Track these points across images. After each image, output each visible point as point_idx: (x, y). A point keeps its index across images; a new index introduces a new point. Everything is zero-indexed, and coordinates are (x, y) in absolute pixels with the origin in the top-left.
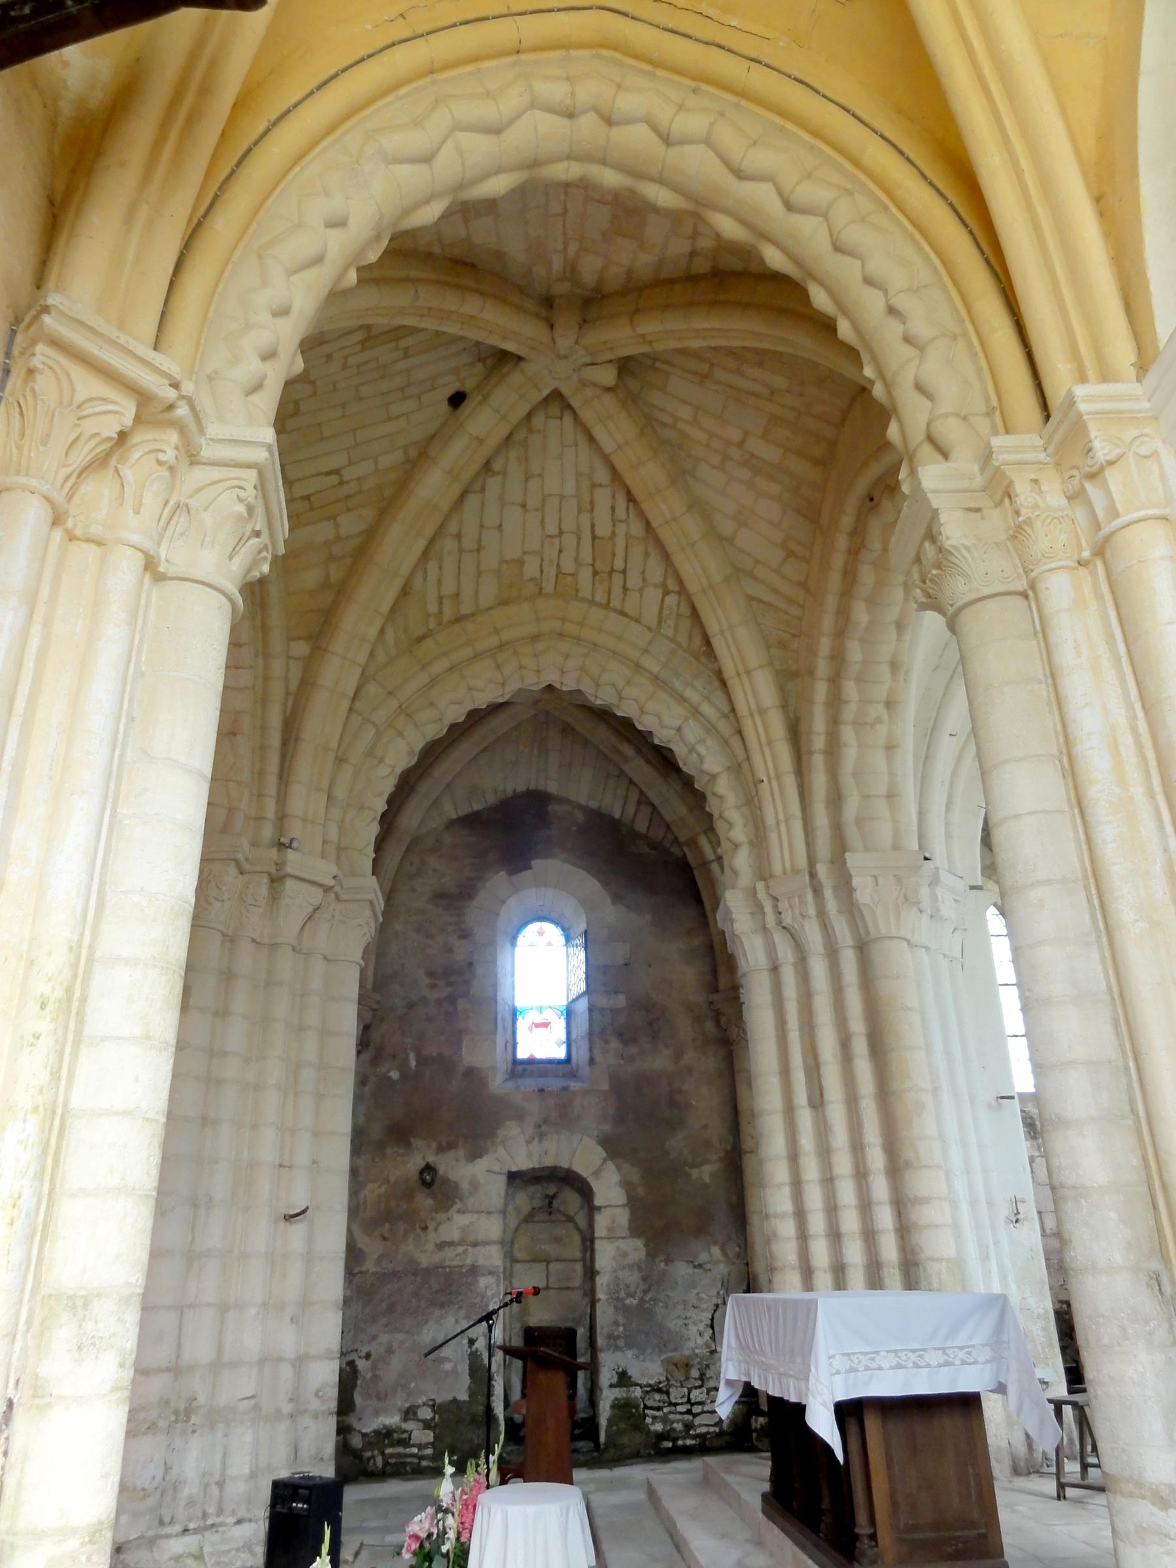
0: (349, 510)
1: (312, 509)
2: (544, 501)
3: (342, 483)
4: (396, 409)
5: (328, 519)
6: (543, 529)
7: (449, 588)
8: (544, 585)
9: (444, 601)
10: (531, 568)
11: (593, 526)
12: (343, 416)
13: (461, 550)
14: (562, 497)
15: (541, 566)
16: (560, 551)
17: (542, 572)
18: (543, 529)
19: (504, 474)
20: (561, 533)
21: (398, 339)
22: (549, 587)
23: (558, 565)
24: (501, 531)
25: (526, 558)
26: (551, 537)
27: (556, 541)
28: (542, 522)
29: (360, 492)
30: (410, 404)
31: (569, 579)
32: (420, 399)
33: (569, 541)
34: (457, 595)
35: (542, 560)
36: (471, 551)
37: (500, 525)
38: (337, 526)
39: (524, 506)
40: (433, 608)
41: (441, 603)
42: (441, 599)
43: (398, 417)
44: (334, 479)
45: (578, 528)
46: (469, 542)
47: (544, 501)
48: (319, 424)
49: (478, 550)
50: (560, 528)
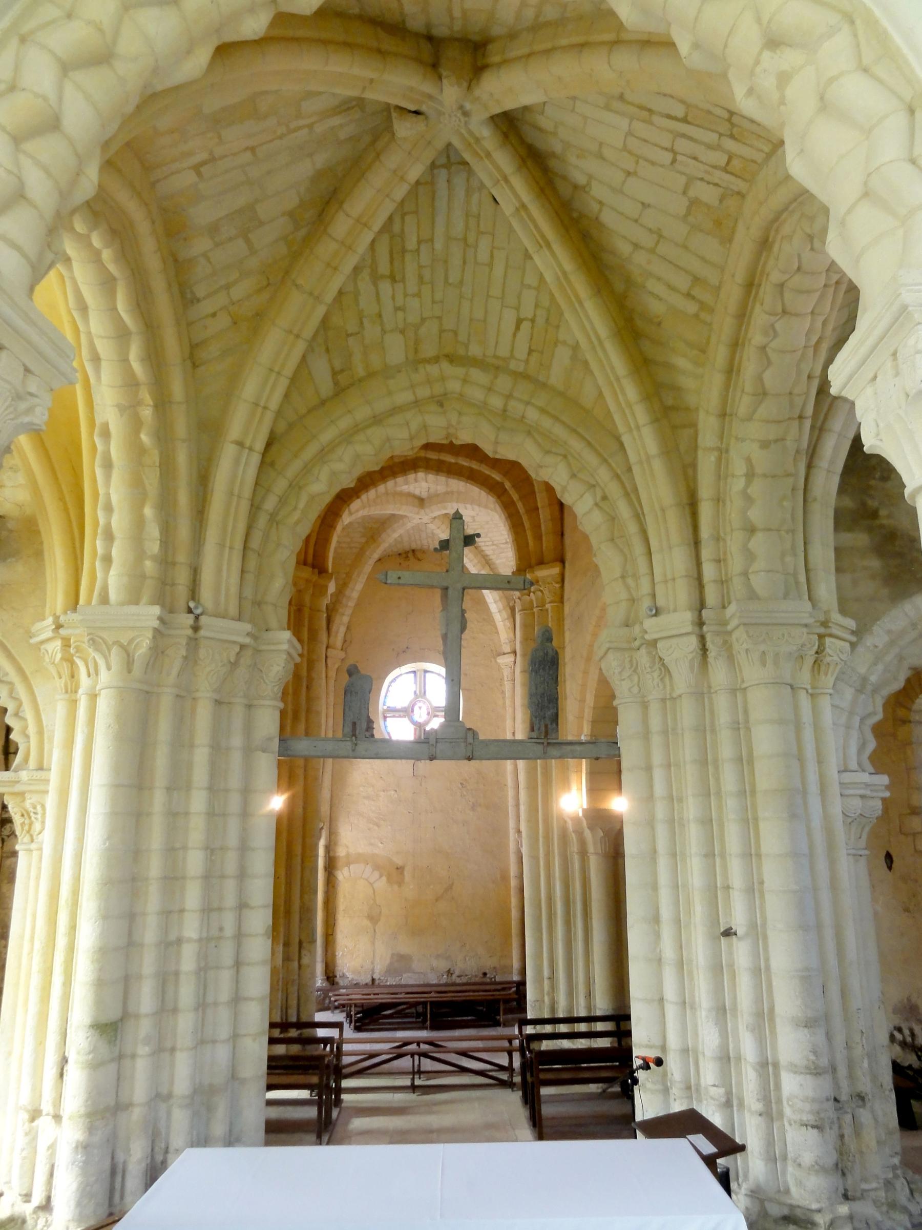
0: (558, 327)
1: (542, 353)
2: (630, 152)
3: (533, 321)
4: (483, 255)
5: (556, 344)
6: (662, 166)
7: (683, 282)
8: (735, 188)
9: (693, 293)
10: (708, 194)
11: (669, 117)
12: (472, 301)
13: (652, 251)
14: (630, 133)
15: (709, 183)
16: (695, 159)
17: (716, 185)
18: (662, 166)
19: (590, 177)
20: (672, 150)
21: (404, 251)
22: (741, 185)
23: (715, 167)
24: (649, 206)
25: (691, 193)
26: (674, 161)
27: (679, 158)
28: (653, 163)
29: (548, 310)
30: (484, 244)
31: (735, 162)
32: (483, 233)
33: (682, 145)
34: (696, 280)
35: (702, 179)
36: (657, 243)
37: (643, 204)
38: (564, 343)
39: (629, 174)
40: (691, 308)
41: (693, 298)
42: (689, 296)
43: (492, 257)
44: (526, 326)
45: (671, 131)
46: (647, 240)
47: (630, 152)
48: (471, 320)
49: (661, 236)
50: (666, 149)
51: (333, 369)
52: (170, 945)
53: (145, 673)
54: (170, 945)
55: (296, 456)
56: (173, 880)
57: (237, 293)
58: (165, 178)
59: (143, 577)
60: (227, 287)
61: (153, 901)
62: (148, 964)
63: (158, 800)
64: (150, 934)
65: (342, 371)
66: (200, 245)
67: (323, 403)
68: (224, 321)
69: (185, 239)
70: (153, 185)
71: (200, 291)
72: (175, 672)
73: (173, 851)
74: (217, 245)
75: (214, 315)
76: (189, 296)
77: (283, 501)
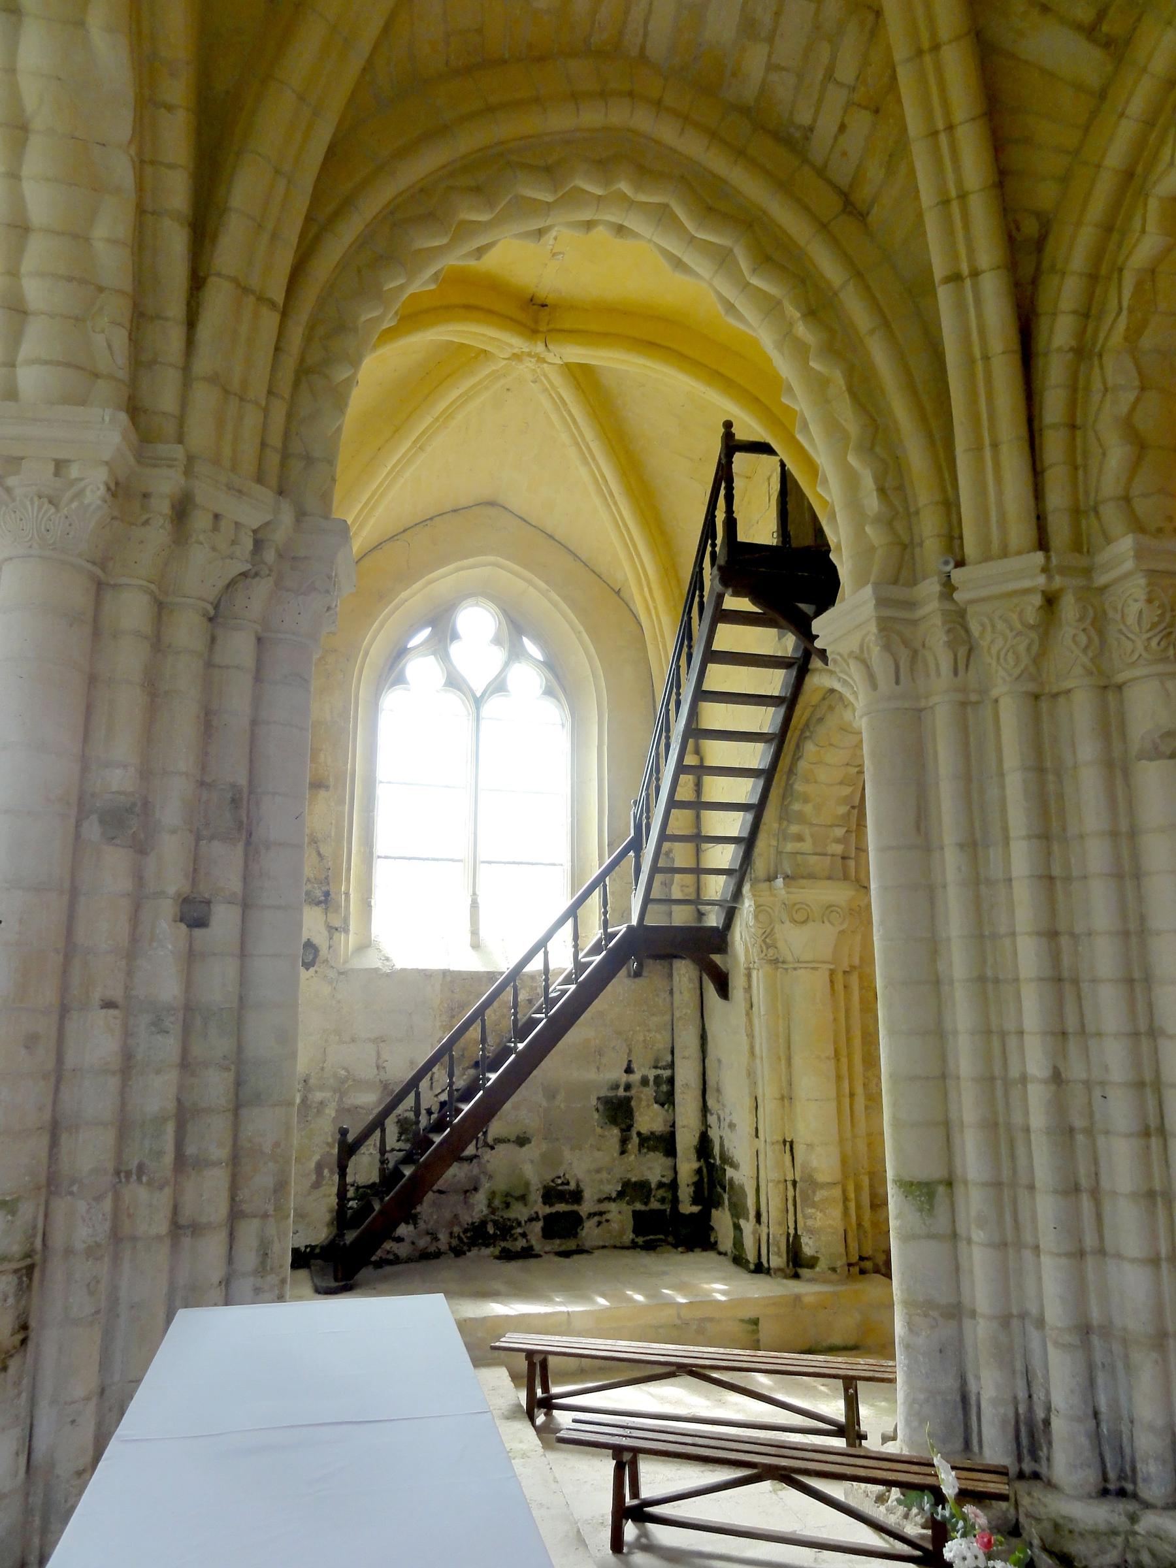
51: (1079, 27)
52: (998, 1083)
53: (897, 682)
54: (998, 1083)
55: (1079, 224)
56: (989, 984)
57: (846, 72)
58: (645, 35)
59: (872, 549)
60: (829, 76)
61: (962, 1015)
62: (968, 1107)
63: (951, 863)
64: (965, 1061)
65: (1101, 15)
66: (755, 60)
67: (1102, 95)
68: (861, 122)
69: (734, 75)
70: (643, 57)
71: (804, 117)
72: (946, 667)
73: (983, 936)
74: (770, 40)
75: (842, 127)
76: (798, 135)
77: (1087, 314)
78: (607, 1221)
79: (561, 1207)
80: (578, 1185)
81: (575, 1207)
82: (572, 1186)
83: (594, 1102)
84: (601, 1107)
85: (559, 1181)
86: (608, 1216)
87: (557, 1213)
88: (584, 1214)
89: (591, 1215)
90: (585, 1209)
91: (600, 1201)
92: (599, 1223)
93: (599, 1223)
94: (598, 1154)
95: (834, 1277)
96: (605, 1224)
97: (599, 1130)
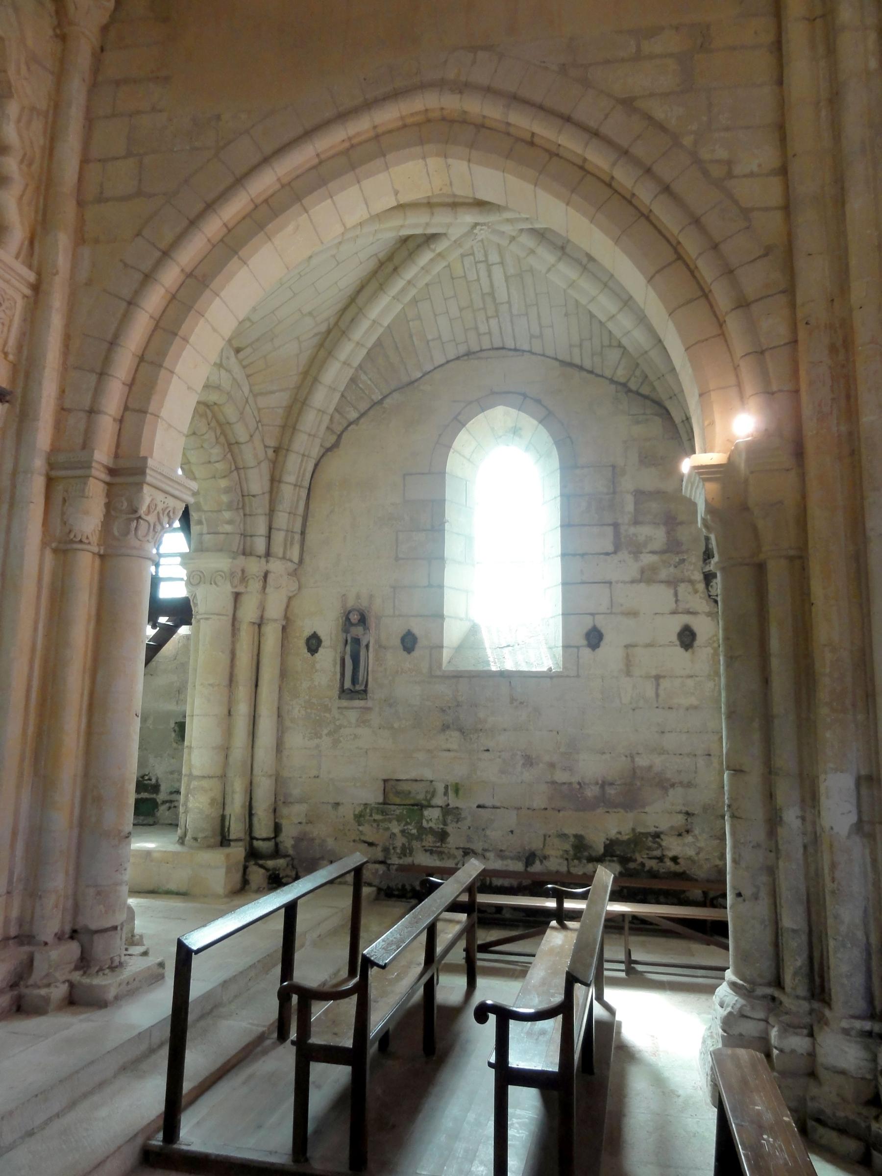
78: (175, 807)
79: (145, 795)
80: (157, 781)
81: (154, 796)
82: (154, 781)
83: (172, 725)
84: (177, 729)
85: (146, 778)
86: (176, 804)
87: (142, 799)
88: (159, 801)
89: (164, 802)
90: (162, 796)
91: (171, 793)
92: (170, 808)
93: (170, 808)
94: (172, 761)
95: (195, 844)
96: (172, 809)
97: (175, 745)
